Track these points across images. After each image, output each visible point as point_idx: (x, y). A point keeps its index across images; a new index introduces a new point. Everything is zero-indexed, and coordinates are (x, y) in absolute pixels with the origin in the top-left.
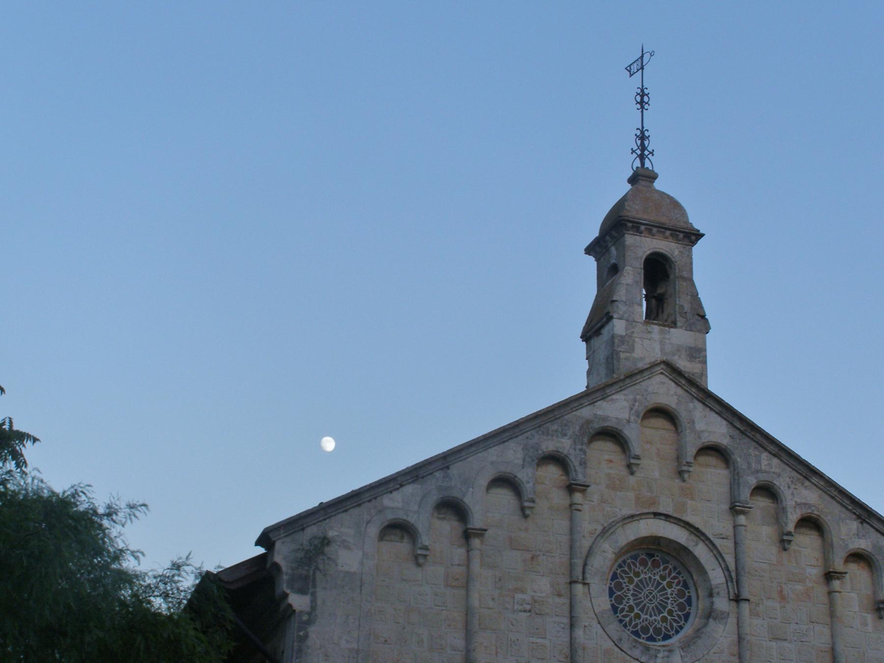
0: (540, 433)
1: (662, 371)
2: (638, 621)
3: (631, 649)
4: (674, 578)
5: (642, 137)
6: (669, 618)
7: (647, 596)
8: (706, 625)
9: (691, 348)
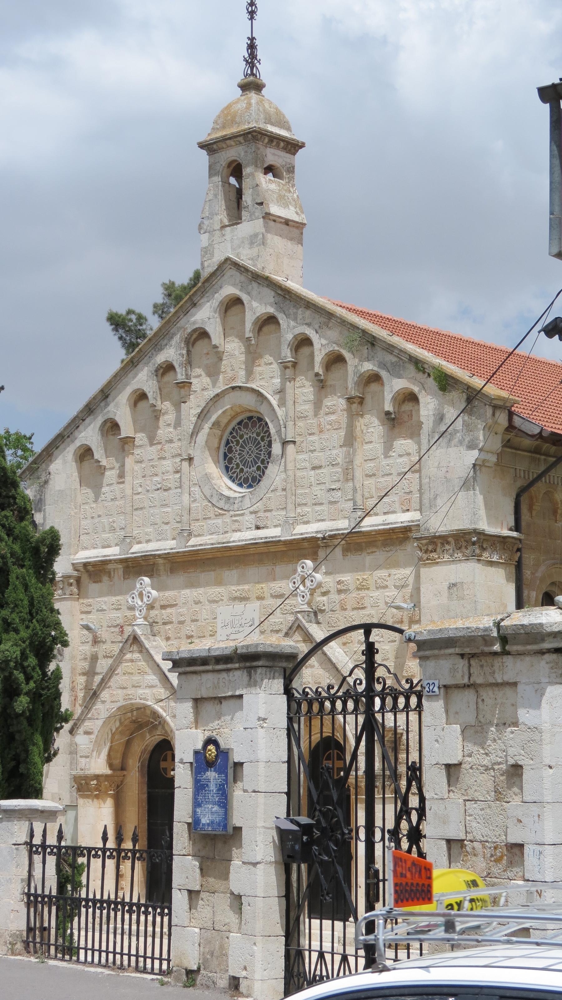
0: (157, 350)
1: (230, 266)
2: (242, 474)
3: (218, 501)
5: (252, 47)
7: (248, 452)
9: (251, 236)
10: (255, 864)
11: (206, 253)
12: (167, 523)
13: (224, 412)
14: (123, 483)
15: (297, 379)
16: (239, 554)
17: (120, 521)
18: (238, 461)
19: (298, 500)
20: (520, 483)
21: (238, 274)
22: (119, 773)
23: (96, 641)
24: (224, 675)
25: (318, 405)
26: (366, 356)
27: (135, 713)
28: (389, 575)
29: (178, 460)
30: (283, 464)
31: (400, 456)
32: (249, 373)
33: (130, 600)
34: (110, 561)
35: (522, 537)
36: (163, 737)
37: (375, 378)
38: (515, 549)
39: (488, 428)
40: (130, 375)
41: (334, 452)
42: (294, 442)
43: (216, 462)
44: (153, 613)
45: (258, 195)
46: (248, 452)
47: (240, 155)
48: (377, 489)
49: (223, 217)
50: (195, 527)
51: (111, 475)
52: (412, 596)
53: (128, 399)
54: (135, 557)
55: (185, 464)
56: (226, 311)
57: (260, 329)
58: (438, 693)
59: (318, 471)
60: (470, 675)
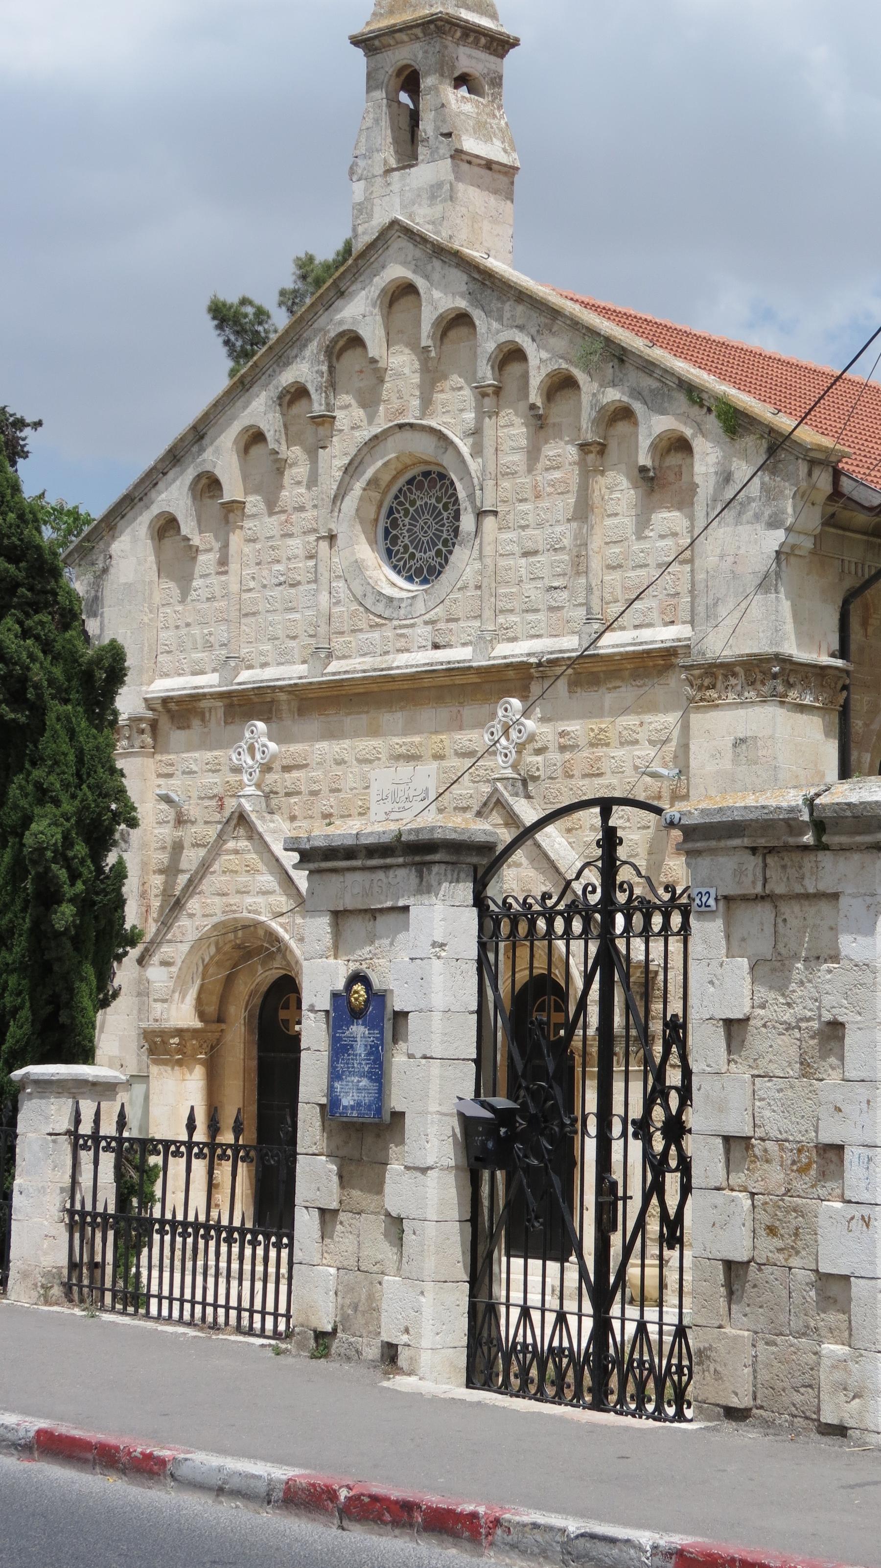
2: (412, 562)
3: (374, 604)
7: (423, 528)
9: (432, 186)
10: (424, 1170)
11: (360, 211)
12: (294, 638)
13: (385, 465)
14: (226, 573)
15: (502, 414)
16: (406, 687)
17: (221, 633)
18: (407, 541)
19: (500, 605)
20: (849, 583)
21: (411, 246)
22: (215, 1026)
23: (180, 821)
24: (381, 875)
25: (533, 454)
26: (611, 378)
27: (240, 933)
28: (641, 724)
29: (312, 538)
30: (476, 547)
31: (663, 537)
32: (426, 402)
33: (234, 757)
34: (204, 695)
35: (851, 667)
36: (284, 972)
37: (624, 414)
38: (839, 686)
39: (801, 496)
40: (239, 404)
41: (558, 529)
42: (495, 513)
43: (372, 542)
44: (270, 778)
45: (444, 121)
46: (423, 528)
47: (415, 56)
48: (625, 588)
49: (388, 155)
50: (338, 643)
51: (206, 561)
52: (676, 757)
53: (236, 442)
54: (244, 690)
55: (324, 545)
56: (391, 304)
57: (444, 334)
58: (714, 908)
59: (532, 559)
60: (765, 880)
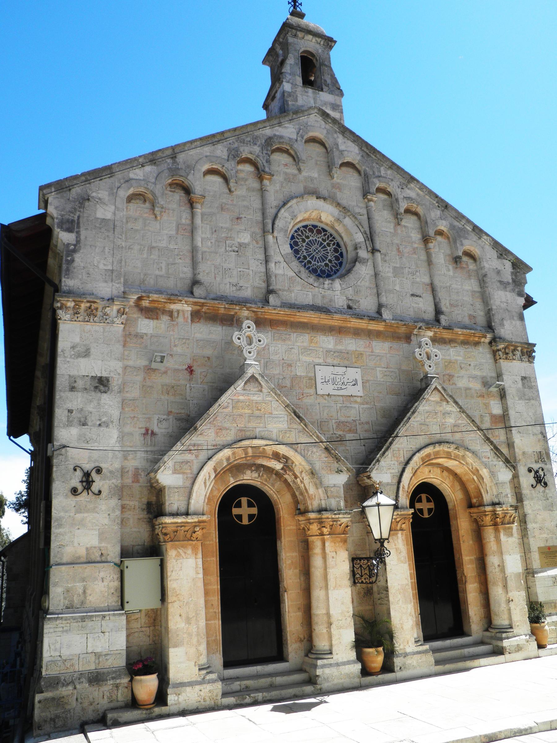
1: (316, 114)
2: (309, 265)
4: (331, 241)
6: (330, 264)
8: (354, 266)
